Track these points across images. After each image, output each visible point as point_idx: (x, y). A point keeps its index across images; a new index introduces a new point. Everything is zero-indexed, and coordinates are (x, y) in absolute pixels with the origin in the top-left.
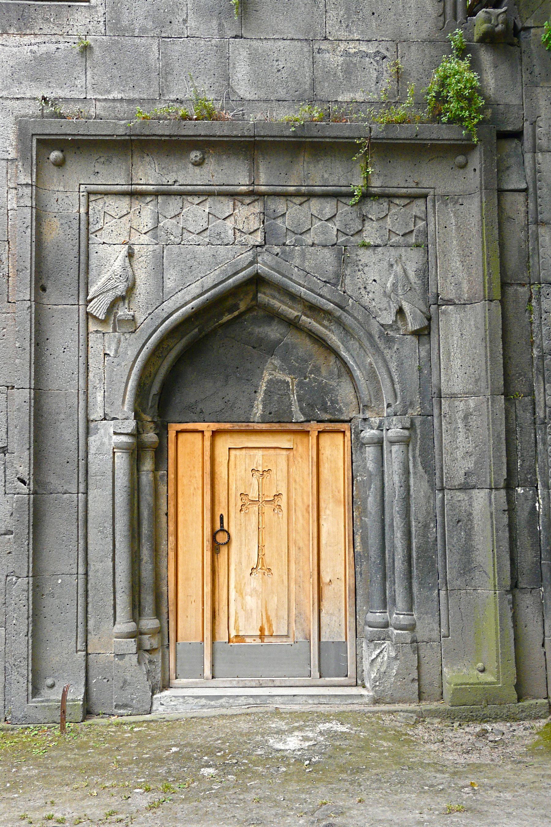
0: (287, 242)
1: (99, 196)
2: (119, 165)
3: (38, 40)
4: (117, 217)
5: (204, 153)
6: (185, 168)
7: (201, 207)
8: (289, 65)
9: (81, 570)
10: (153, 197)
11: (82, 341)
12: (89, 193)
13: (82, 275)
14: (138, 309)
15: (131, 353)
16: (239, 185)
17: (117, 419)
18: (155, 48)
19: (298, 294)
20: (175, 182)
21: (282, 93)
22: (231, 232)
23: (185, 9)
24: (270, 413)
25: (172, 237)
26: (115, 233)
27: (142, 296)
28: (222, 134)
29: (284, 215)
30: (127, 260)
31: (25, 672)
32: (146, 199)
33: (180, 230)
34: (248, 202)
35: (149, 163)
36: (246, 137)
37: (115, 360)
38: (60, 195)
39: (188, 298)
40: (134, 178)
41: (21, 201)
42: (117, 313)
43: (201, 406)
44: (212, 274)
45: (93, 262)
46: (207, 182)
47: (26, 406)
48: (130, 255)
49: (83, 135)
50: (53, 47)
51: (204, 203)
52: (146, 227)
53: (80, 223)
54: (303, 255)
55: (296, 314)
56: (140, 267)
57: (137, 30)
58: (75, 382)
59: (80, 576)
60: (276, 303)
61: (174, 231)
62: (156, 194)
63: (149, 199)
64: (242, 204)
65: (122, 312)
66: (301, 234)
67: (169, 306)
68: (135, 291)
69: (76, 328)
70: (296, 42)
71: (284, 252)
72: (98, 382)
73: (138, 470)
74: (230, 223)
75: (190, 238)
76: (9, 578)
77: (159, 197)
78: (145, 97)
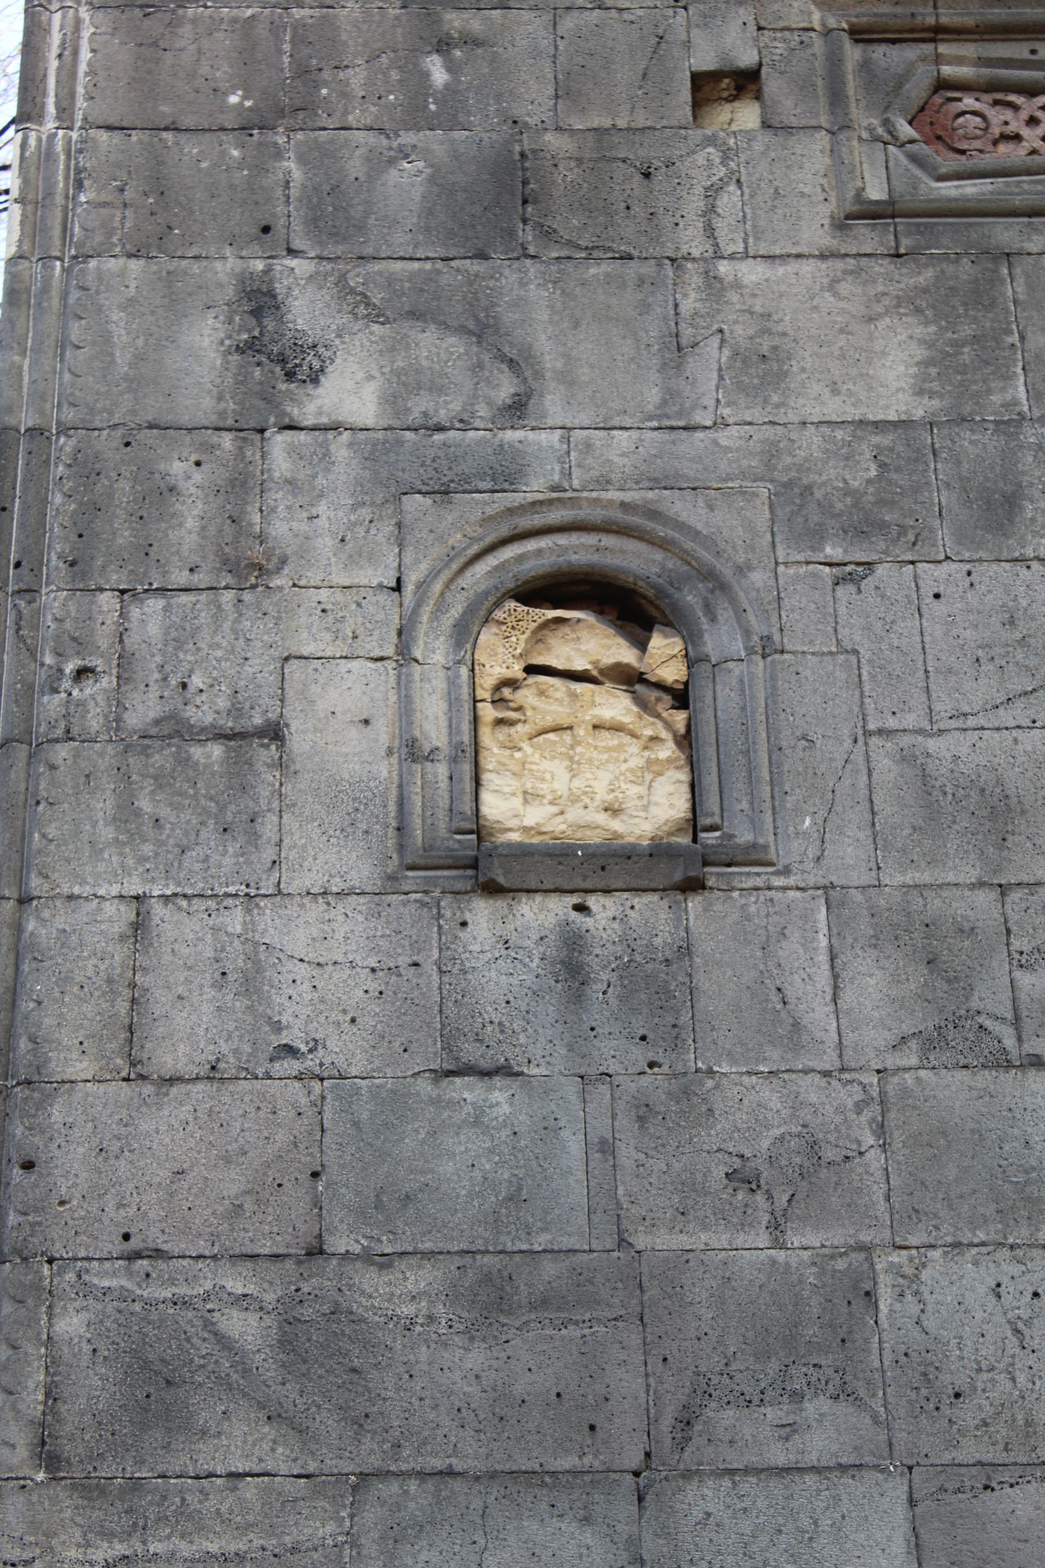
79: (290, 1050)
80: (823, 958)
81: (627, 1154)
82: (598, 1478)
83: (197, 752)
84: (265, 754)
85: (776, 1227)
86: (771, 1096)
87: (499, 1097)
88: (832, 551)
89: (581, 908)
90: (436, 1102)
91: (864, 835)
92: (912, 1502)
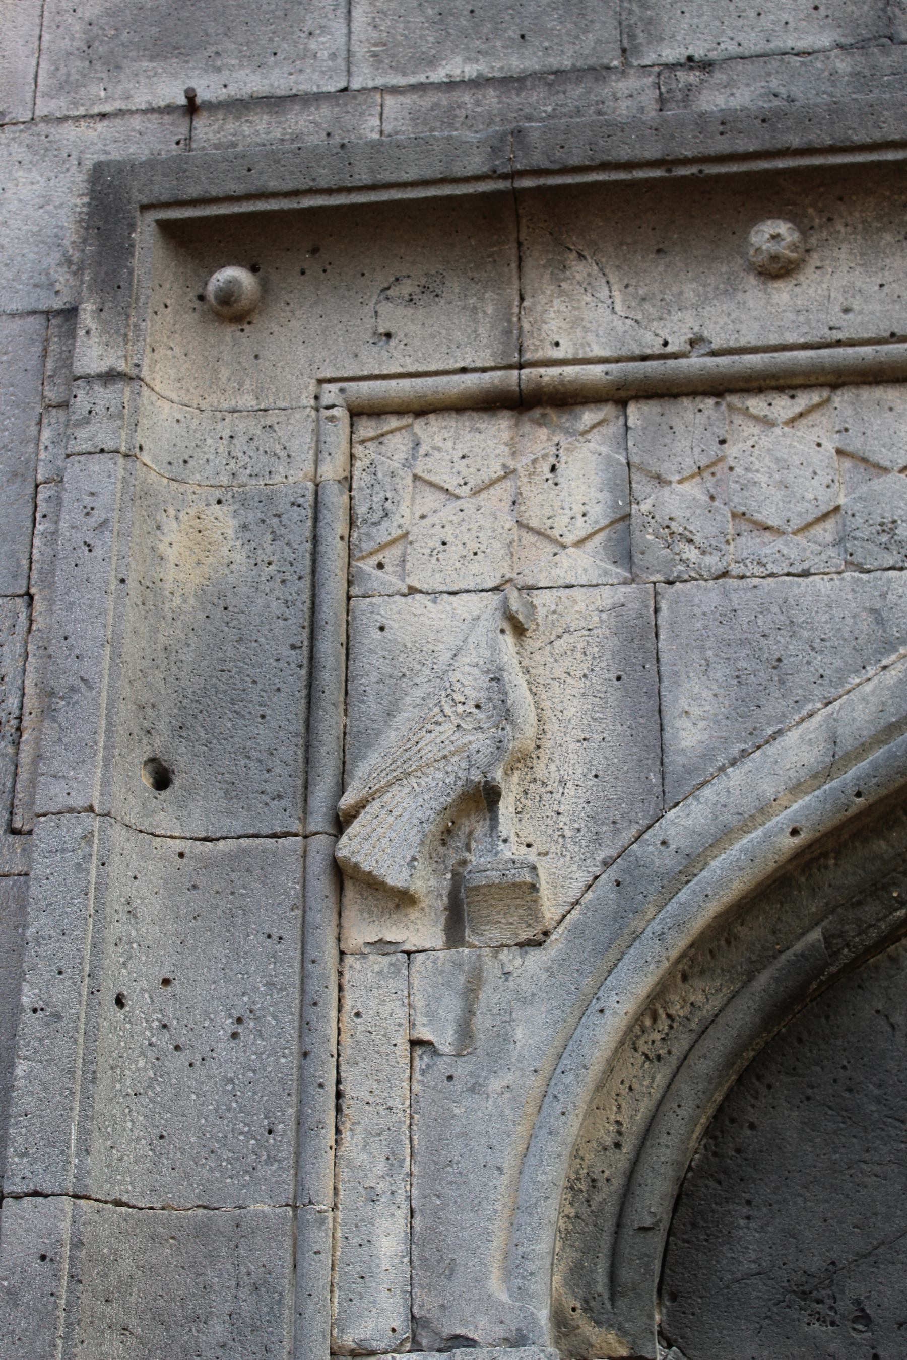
1: (394, 422)
2: (472, 301)
4: (464, 491)
5: (806, 230)
6: (731, 288)
10: (608, 410)
12: (357, 413)
15: (530, 1033)
17: (468, 1342)
20: (692, 343)
25: (691, 553)
26: (455, 550)
27: (571, 790)
28: (877, 136)
30: (508, 641)
32: (578, 418)
35: (588, 287)
37: (461, 1069)
38: (242, 425)
40: (528, 342)
41: (82, 433)
42: (464, 863)
43: (854, 1288)
44: (868, 688)
45: (371, 666)
46: (822, 333)
49: (329, 192)
51: (815, 416)
52: (580, 521)
53: (316, 520)
56: (559, 672)
61: (703, 528)
62: (621, 395)
63: (589, 417)
69: (291, 934)
72: (380, 1167)
75: (767, 550)
77: (632, 409)
78: (567, 64)
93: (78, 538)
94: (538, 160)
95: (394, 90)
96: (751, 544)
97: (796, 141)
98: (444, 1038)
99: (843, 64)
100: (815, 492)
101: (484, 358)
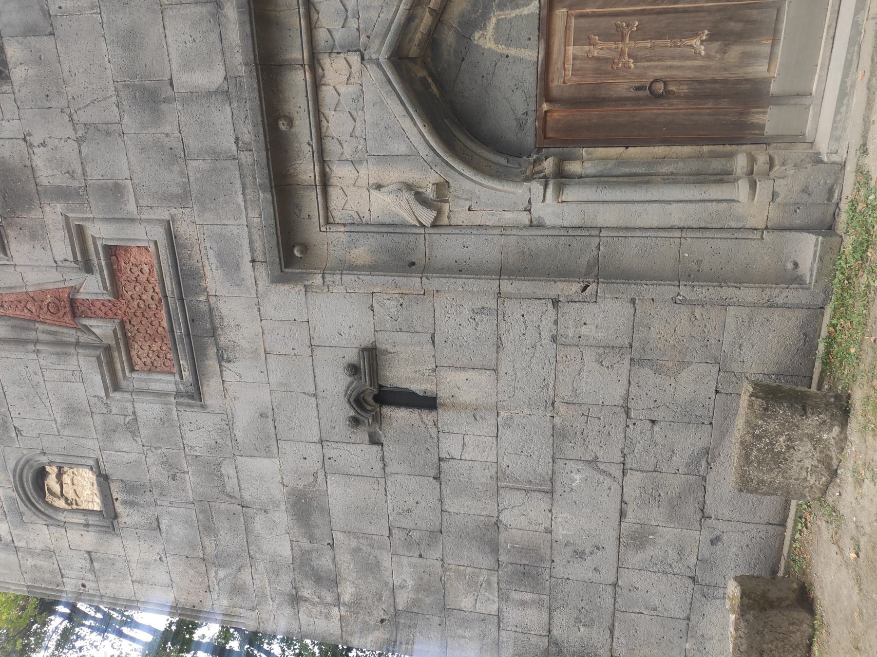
0: (356, 26)
3: (207, 264)
7: (331, 119)
8: (187, 30)
9: (677, 234)
11: (457, 231)
13: (398, 231)
14: (427, 181)
15: (468, 185)
16: (305, 80)
18: (194, 163)
19: (407, 12)
21: (214, 37)
22: (351, 88)
23: (157, 135)
24: (529, 39)
25: (360, 147)
29: (329, 31)
31: (777, 291)
33: (353, 139)
34: (320, 70)
35: (296, 169)
36: (257, 75)
37: (475, 200)
39: (415, 131)
43: (520, 114)
45: (387, 219)
47: (516, 283)
48: (379, 187)
50: (210, 252)
54: (368, 8)
55: (427, 14)
57: (184, 180)
58: (495, 238)
59: (684, 235)
60: (418, 37)
63: (328, 169)
64: (323, 76)
65: (430, 193)
66: (347, 11)
67: (423, 151)
68: (411, 182)
70: (166, 23)
71: (366, 30)
73: (580, 177)
74: (342, 89)
76: (678, 301)
79: (160, 559)
80: (119, 453)
81: (172, 499)
82: (245, 515)
83: (96, 568)
84: (94, 555)
85: (184, 472)
86: (153, 469)
87: (164, 522)
88: (14, 435)
89: (117, 499)
90: (167, 534)
91: (86, 440)
92: (241, 456)
93: (361, 283)
94: (267, 181)
95: (247, 214)
96: (358, 133)
97: (260, 118)
98: (468, 203)
99: (235, 105)
100: (344, 117)
101: (314, 193)
